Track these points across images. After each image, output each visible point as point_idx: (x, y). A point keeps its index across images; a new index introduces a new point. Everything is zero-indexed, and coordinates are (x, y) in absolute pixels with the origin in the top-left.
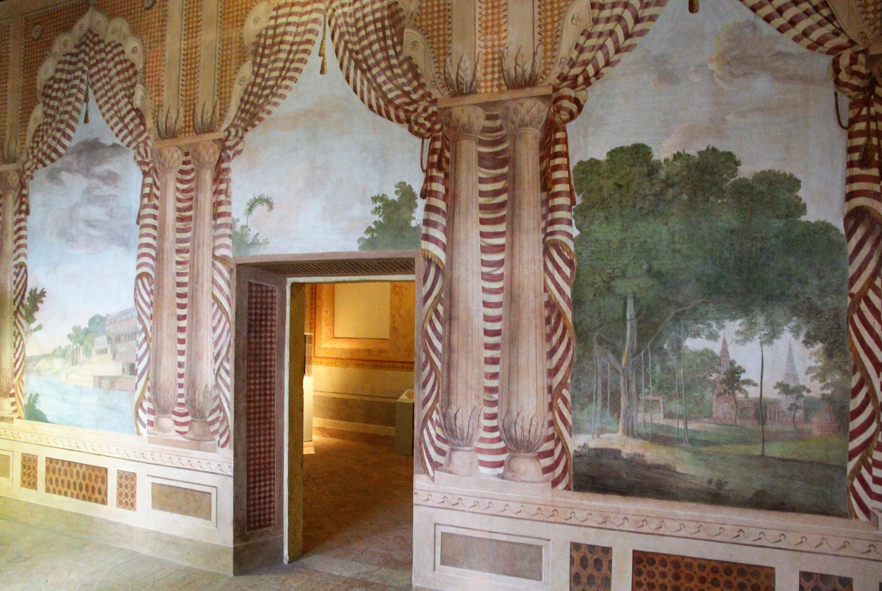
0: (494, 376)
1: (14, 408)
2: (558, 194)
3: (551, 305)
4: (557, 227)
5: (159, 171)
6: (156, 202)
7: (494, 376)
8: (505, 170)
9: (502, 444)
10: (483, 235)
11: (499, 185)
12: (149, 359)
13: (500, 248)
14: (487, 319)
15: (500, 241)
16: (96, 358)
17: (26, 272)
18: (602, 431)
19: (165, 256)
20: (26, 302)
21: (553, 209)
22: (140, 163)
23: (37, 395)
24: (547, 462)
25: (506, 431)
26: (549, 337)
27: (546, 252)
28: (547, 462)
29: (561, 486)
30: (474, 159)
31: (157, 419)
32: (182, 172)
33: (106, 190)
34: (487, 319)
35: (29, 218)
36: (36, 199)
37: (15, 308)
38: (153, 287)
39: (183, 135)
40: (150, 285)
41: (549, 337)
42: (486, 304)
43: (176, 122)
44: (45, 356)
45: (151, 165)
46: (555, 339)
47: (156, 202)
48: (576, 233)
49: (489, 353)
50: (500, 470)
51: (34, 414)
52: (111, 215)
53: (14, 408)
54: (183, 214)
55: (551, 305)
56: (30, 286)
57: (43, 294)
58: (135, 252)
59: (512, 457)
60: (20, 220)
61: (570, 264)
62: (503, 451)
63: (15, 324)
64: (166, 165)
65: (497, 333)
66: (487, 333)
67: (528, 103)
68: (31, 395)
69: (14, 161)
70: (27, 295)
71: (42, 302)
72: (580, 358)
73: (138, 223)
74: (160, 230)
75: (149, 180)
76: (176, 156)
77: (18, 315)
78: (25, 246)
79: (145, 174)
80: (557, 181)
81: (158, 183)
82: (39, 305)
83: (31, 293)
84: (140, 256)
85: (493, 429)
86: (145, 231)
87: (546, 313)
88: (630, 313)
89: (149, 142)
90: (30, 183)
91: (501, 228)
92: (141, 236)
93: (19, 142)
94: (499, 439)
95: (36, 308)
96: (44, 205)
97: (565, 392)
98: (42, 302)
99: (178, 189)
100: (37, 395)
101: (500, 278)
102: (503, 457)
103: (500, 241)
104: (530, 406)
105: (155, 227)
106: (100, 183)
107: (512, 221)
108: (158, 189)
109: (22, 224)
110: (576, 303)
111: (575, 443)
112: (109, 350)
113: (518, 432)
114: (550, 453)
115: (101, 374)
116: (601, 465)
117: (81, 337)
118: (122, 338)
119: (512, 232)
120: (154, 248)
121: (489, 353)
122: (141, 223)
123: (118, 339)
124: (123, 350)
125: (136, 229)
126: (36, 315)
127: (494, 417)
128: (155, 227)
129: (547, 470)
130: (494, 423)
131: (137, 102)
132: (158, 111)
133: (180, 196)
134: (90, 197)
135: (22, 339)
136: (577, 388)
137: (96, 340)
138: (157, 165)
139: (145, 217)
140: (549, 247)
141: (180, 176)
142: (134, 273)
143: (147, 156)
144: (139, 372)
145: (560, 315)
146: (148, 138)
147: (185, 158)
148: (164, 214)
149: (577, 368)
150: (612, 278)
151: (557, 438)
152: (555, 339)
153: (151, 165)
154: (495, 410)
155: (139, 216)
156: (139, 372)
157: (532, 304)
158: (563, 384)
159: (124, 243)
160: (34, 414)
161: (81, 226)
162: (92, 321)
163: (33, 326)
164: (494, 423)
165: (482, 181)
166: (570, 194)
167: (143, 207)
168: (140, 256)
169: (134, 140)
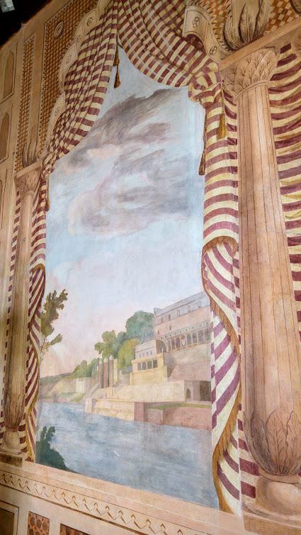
1: (24, 445)
5: (232, 94)
6: (233, 135)
12: (238, 373)
16: (138, 375)
17: (44, 274)
19: (260, 204)
20: (42, 310)
22: (198, 98)
23: (53, 429)
31: (264, 484)
32: (277, 77)
33: (147, 149)
35: (49, 214)
36: (57, 191)
37: (29, 319)
38: (237, 256)
39: (274, 27)
40: (232, 254)
43: (257, 18)
44: (63, 376)
45: (218, 92)
47: (233, 135)
51: (51, 459)
52: (156, 177)
53: (24, 445)
54: (288, 133)
56: (48, 290)
57: (64, 296)
58: (200, 212)
60: (38, 220)
63: (29, 338)
64: (246, 79)
68: (45, 428)
69: (34, 161)
70: (44, 301)
71: (62, 307)
73: (201, 173)
74: (246, 173)
75: (218, 111)
76: (263, 61)
77: (33, 327)
78: (44, 245)
79: (208, 107)
81: (233, 109)
82: (58, 311)
83: (49, 298)
84: (206, 218)
86: (214, 179)
89: (213, 66)
90: (50, 177)
92: (209, 188)
93: (40, 140)
95: (54, 315)
96: (66, 194)
98: (62, 307)
99: (272, 103)
100: (53, 429)
105: (234, 170)
106: (139, 144)
108: (234, 117)
109: (41, 223)
112: (161, 362)
115: (149, 399)
117: (115, 347)
118: (183, 342)
120: (236, 198)
122: (207, 171)
123: (176, 344)
124: (185, 360)
125: (201, 182)
126: (54, 324)
128: (234, 170)
131: (188, 28)
132: (225, 21)
133: (277, 110)
134: (125, 166)
135: (36, 356)
137: (139, 348)
138: (229, 88)
139: (214, 160)
141: (275, 84)
142: (199, 243)
143: (210, 83)
144: (218, 396)
146: (210, 61)
147: (282, 56)
148: (250, 144)
153: (218, 92)
155: (203, 163)
156: (218, 396)
159: (181, 206)
160: (51, 459)
161: (114, 203)
162: (131, 322)
163: (50, 338)
167: (208, 149)
168: (206, 218)
169: (187, 75)
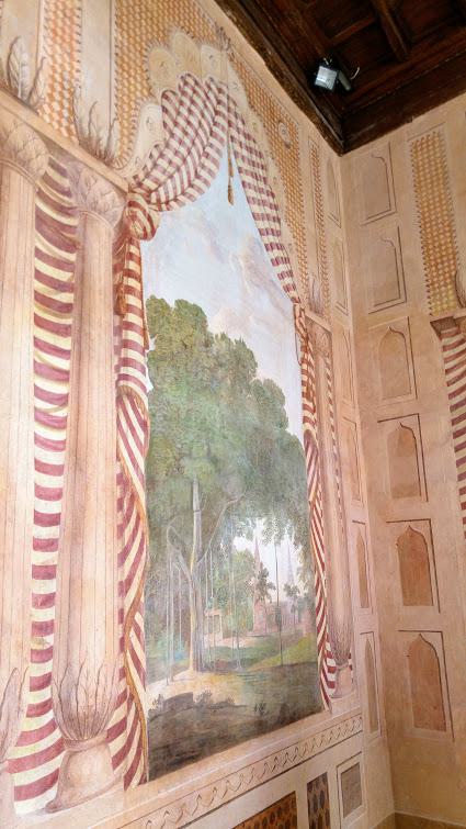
0: (48, 600)
2: (129, 326)
3: (123, 480)
4: (130, 371)
7: (48, 600)
8: (72, 257)
9: (57, 735)
10: (38, 343)
11: (64, 276)
13: (63, 376)
14: (41, 493)
15: (63, 364)
18: (176, 669)
21: (126, 344)
24: (117, 744)
25: (64, 704)
26: (121, 529)
27: (119, 400)
28: (117, 744)
29: (135, 781)
30: (31, 219)
34: (41, 493)
41: (121, 529)
42: (40, 467)
46: (128, 532)
48: (150, 387)
49: (41, 558)
50: (51, 794)
55: (123, 480)
59: (72, 755)
61: (144, 425)
62: (58, 748)
65: (53, 520)
66: (41, 519)
67: (102, 185)
72: (153, 561)
80: (129, 308)
85: (44, 708)
87: (118, 492)
88: (196, 505)
91: (65, 343)
94: (52, 726)
97: (139, 618)
101: (59, 424)
102: (57, 762)
103: (63, 364)
104: (95, 647)
107: (79, 334)
110: (150, 482)
111: (151, 696)
113: (81, 703)
114: (121, 726)
116: (176, 723)
119: (79, 354)
121: (41, 558)
127: (44, 682)
129: (119, 758)
130: (45, 694)
136: (151, 608)
140: (123, 396)
145: (133, 497)
149: (151, 578)
150: (182, 456)
151: (129, 697)
152: (128, 532)
154: (48, 667)
157: (101, 474)
158: (135, 605)
164: (45, 694)
165: (38, 253)
166: (143, 332)
